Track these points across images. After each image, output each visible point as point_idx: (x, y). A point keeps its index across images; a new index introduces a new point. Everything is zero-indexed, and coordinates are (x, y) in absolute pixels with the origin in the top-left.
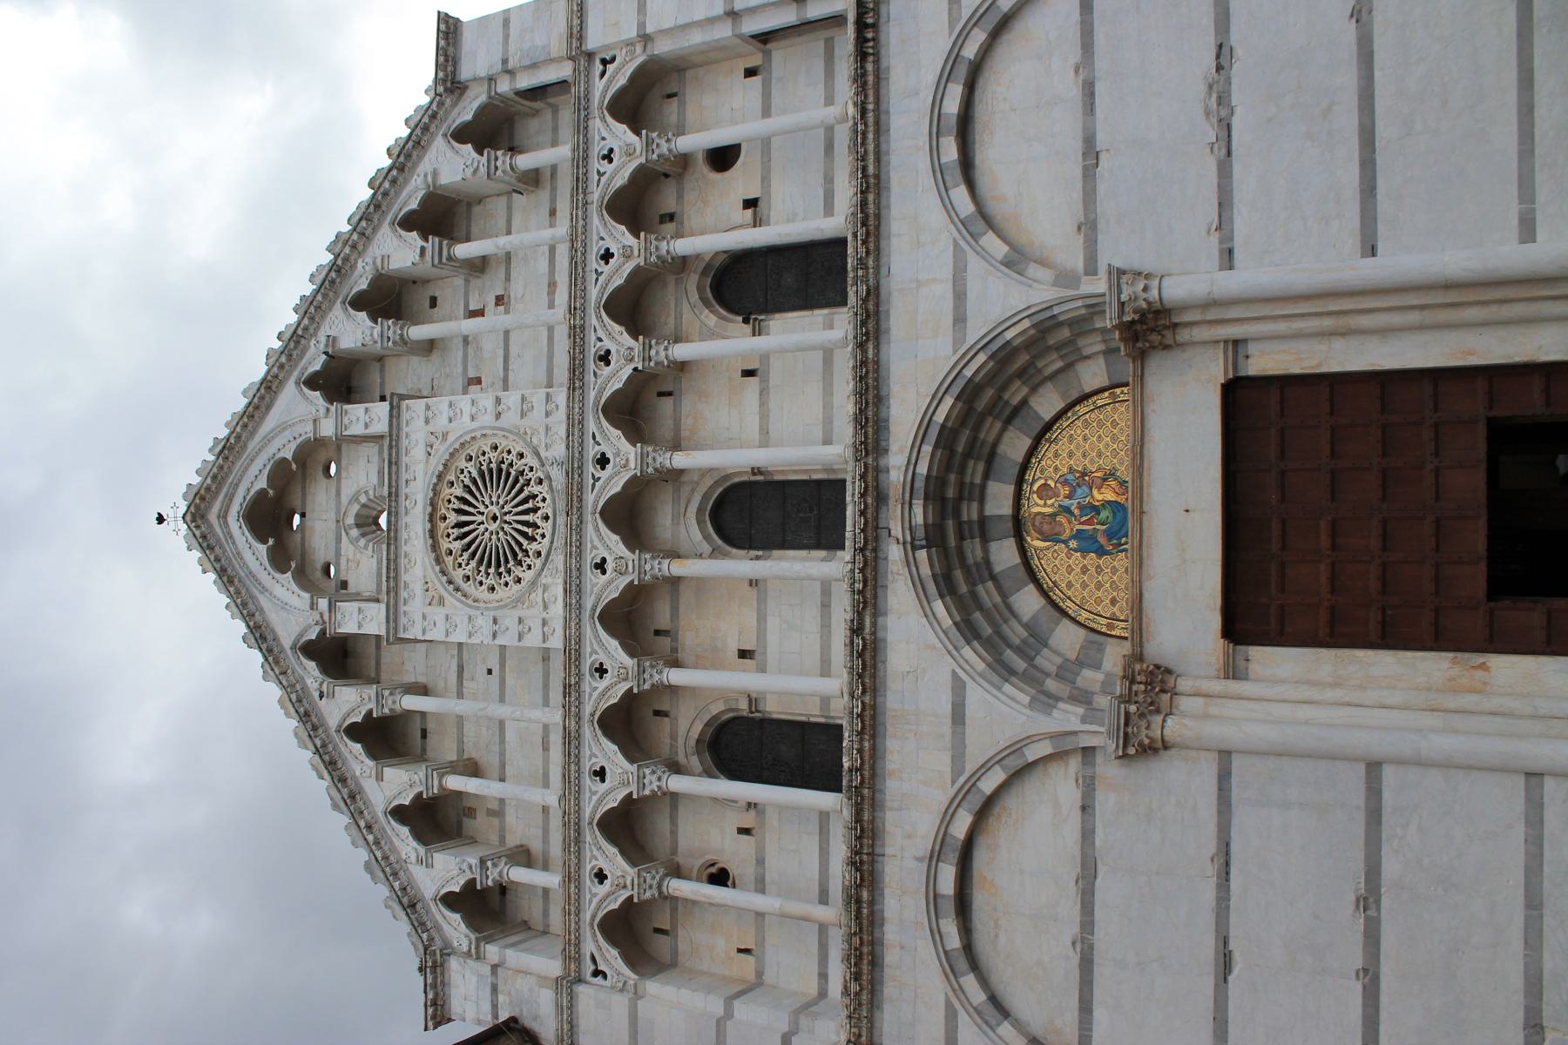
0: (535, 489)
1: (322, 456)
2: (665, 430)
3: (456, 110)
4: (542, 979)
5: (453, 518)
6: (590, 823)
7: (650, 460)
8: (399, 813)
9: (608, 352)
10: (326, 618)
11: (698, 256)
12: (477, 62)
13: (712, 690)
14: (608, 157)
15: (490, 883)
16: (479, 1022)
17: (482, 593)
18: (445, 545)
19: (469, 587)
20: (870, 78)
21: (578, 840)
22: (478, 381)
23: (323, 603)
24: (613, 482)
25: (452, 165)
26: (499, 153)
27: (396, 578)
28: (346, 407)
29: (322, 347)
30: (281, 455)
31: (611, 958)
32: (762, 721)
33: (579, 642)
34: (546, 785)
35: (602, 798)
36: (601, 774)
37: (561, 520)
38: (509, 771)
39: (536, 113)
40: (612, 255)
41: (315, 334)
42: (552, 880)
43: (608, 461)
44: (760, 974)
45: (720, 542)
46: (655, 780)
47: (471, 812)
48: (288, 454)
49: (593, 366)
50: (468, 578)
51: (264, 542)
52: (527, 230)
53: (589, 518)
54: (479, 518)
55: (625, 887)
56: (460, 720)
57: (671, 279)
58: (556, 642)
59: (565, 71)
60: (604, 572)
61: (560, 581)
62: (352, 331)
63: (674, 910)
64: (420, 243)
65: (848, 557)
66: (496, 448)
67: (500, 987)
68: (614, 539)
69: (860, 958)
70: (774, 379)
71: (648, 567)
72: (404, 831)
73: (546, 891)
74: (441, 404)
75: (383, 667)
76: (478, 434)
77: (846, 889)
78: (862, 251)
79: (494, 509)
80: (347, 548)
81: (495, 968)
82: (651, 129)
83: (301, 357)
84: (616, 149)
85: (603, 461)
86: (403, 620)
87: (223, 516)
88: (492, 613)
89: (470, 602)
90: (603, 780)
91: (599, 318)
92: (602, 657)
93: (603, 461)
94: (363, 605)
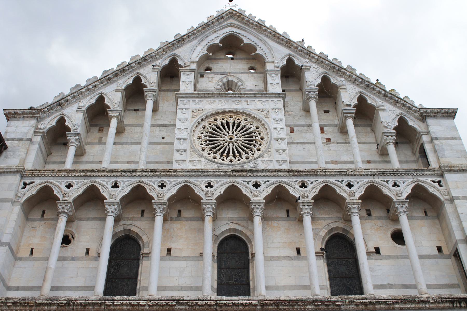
0: (244, 156)
1: (257, 66)
2: (272, 213)
3: (413, 118)
4: (24, 160)
5: (231, 121)
6: (93, 182)
7: (257, 206)
8: (101, 99)
9: (306, 187)
10: (187, 68)
11: (351, 227)
12: (436, 126)
13: (153, 236)
14: (395, 185)
15: (68, 138)
16: (6, 133)
17: (198, 134)
18: (219, 118)
19: (200, 128)
20: (441, 305)
21: (86, 176)
22: (292, 131)
23: (193, 67)
24: (247, 190)
25: (388, 117)
26: (394, 137)
27: (204, 97)
28: (279, 75)
29: (306, 64)
30: (258, 49)
31: (31, 191)
32: (139, 259)
33: (175, 176)
34: (111, 163)
35: (105, 187)
36: (116, 186)
37: (230, 168)
38: (119, 147)
39: (414, 154)
40: (350, 188)
41: (311, 61)
42: (69, 165)
43: (257, 188)
44: (21, 259)
45: (221, 239)
46: (112, 210)
47: (101, 130)
48: (259, 51)
49: (299, 180)
50: (204, 128)
51: (220, 42)
52: (360, 151)
53: (231, 179)
54: (231, 132)
55: (64, 197)
56: (141, 126)
57: (340, 215)
58: (175, 166)
59: (434, 164)
60: (206, 187)
61: (203, 168)
62: (313, 77)
63: (53, 220)
64: (353, 104)
65: (213, 298)
66: (262, 139)
67: (21, 142)
68: (221, 191)
69: (24, 305)
70: (295, 263)
71: (209, 206)
72: (93, 101)
73: (64, 163)
74: (281, 115)
75: (166, 93)
76: (268, 131)
77: (57, 298)
78: (358, 302)
79: (235, 139)
80: (218, 77)
81: (30, 140)
82: (409, 203)
83: (301, 56)
84: (399, 188)
85: (257, 185)
86: (186, 100)
87: (232, 25)
88: (188, 138)
89: (194, 129)
90: (113, 187)
91: (322, 183)
92: (168, 186)
93: (257, 185)
94: (193, 84)
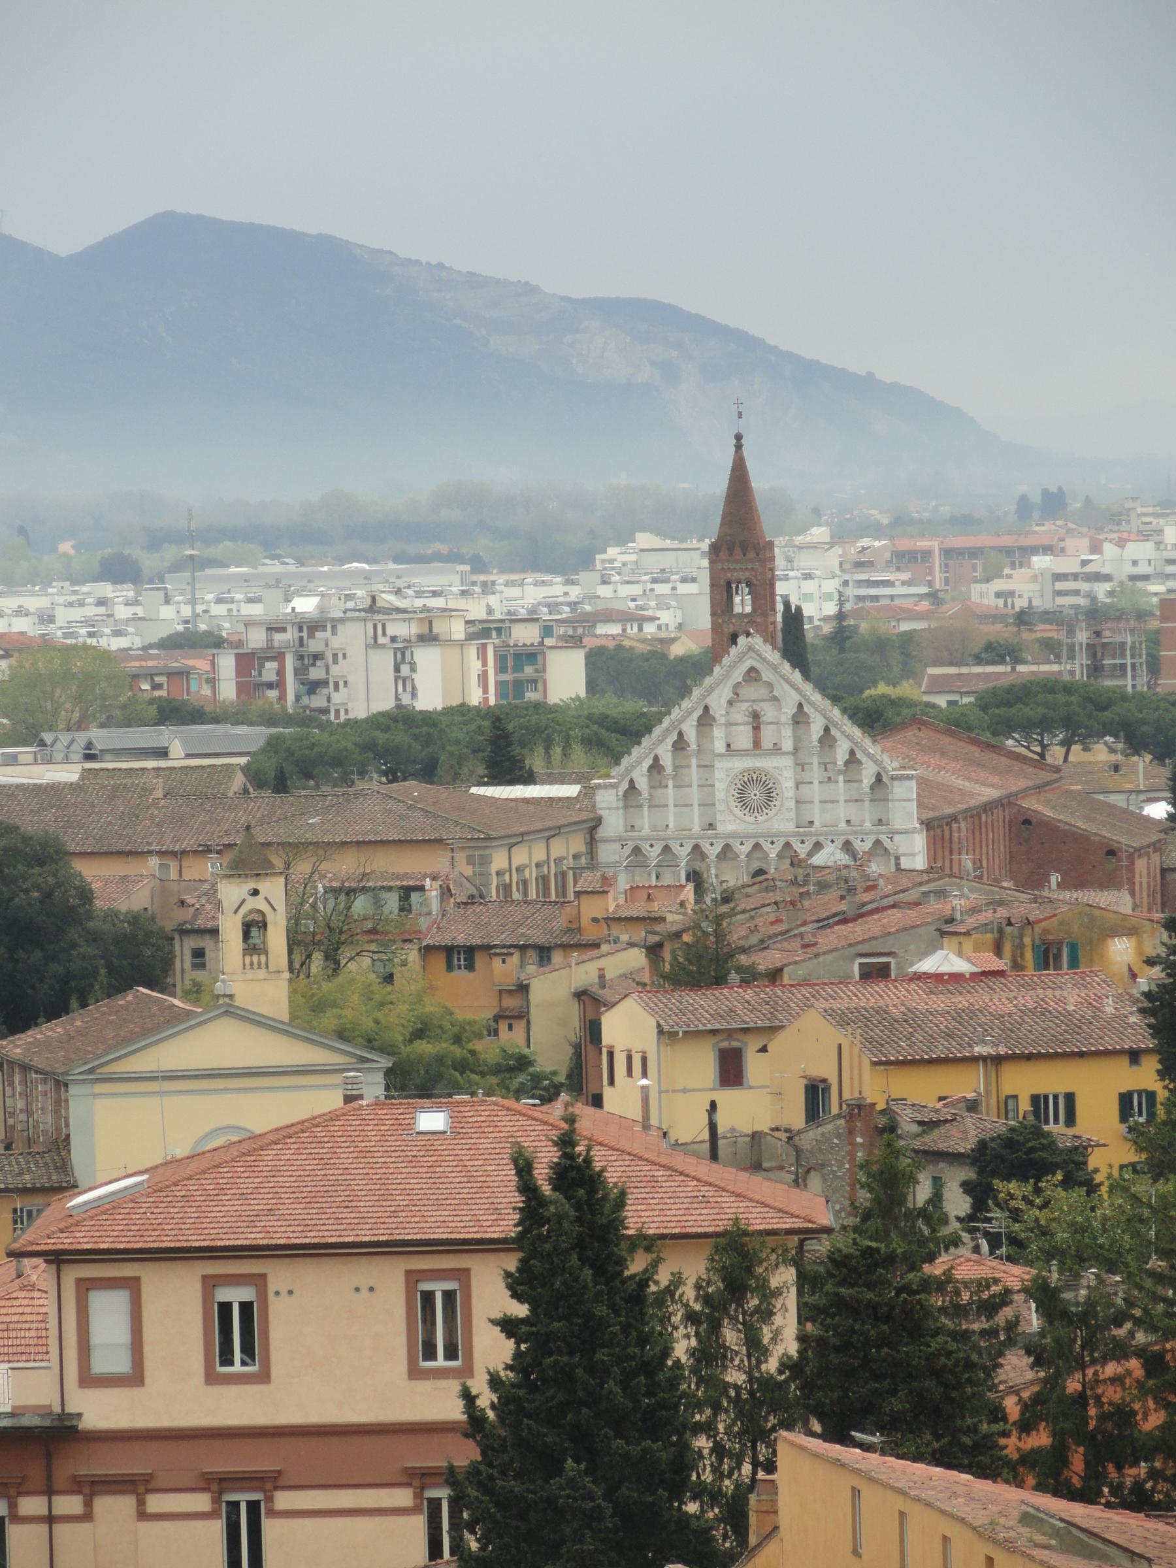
19: (733, 787)
31: (628, 850)
85: (772, 843)
